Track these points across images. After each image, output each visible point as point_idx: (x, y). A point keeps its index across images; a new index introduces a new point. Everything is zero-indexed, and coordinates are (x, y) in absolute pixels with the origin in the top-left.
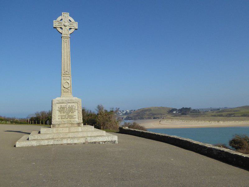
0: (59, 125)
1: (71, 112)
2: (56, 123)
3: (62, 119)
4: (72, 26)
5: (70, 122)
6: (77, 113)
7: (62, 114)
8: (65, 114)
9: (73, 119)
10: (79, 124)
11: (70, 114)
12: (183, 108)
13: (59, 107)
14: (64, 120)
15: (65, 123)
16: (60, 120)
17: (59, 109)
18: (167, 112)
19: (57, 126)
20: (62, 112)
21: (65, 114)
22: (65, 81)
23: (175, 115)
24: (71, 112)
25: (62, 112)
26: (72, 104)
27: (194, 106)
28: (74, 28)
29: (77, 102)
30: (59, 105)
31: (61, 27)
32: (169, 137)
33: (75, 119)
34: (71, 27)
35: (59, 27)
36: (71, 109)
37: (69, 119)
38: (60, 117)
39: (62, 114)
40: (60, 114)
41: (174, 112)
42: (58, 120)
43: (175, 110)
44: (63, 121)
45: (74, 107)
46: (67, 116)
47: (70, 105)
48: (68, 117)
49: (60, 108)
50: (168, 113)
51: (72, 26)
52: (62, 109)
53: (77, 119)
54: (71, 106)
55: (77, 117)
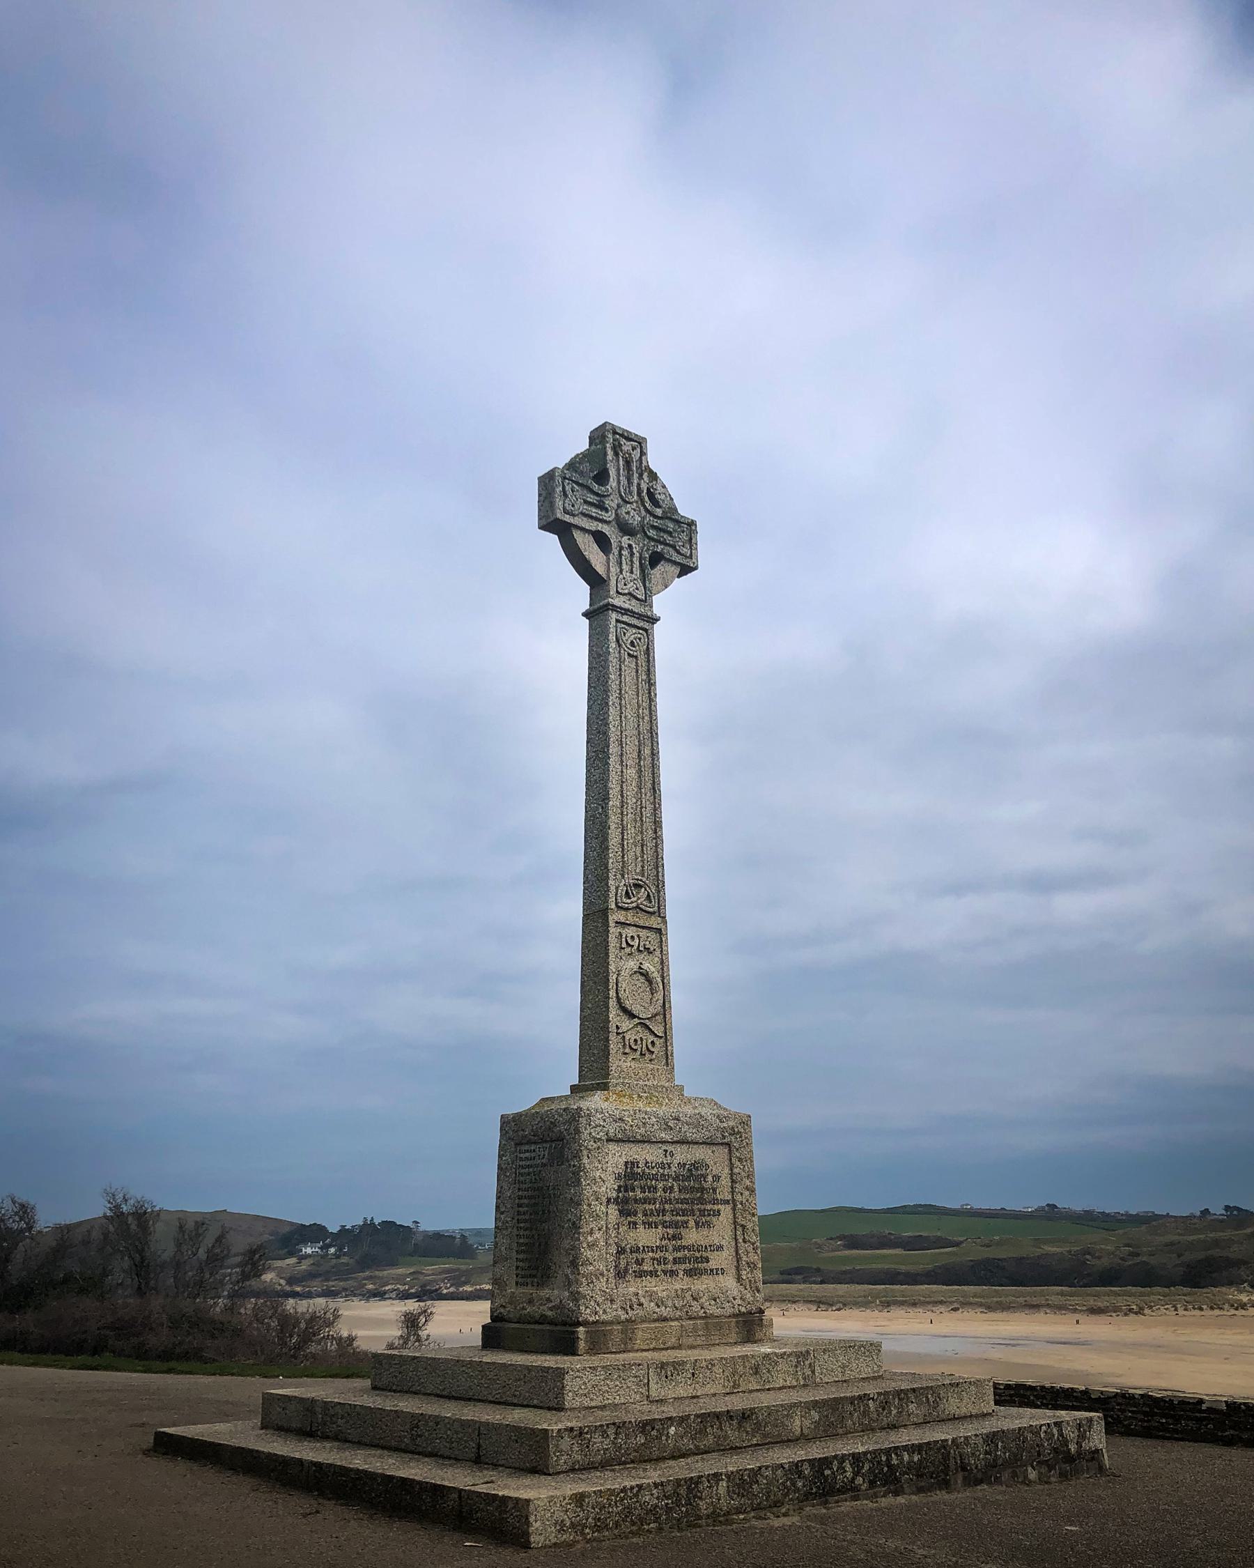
1: (691, 1223)
11: (692, 1236)
15: (664, 1311)
24: (691, 1223)
26: (700, 1153)
30: (617, 1157)
37: (680, 1283)
43: (315, 1233)
44: (651, 1295)
53: (729, 1282)
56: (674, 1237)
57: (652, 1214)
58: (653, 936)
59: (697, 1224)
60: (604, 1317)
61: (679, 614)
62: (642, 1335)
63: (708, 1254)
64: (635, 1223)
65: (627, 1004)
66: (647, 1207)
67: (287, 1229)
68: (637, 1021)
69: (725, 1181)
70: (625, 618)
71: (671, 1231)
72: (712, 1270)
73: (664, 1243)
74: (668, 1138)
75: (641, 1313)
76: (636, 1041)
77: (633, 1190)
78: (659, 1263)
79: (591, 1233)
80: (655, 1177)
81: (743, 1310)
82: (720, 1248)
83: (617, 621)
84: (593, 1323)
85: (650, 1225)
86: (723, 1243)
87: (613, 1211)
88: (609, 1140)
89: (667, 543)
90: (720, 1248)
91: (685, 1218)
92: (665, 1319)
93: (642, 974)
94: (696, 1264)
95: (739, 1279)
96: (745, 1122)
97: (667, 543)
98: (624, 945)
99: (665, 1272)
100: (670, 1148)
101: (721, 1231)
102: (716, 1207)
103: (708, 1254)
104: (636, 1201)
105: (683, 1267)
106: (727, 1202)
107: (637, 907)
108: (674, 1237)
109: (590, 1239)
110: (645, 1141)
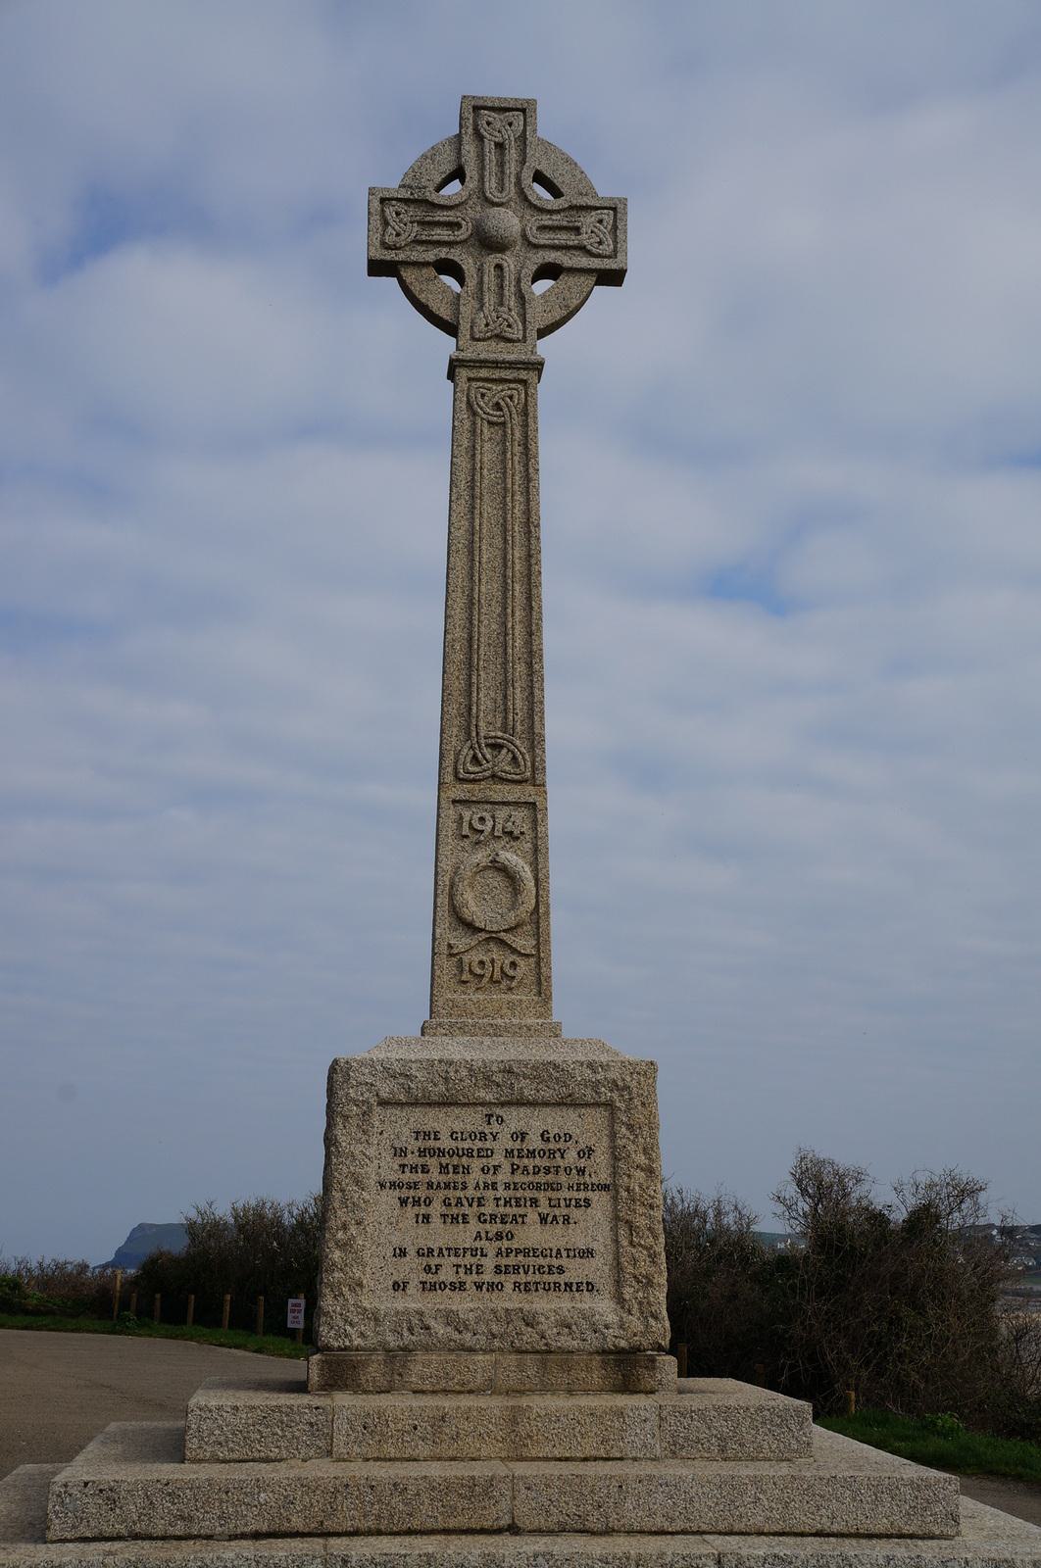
0: (397, 1357)
1: (532, 1216)
2: (372, 1341)
3: (433, 1287)
4: (570, 239)
5: (529, 1337)
6: (606, 1227)
7: (439, 1234)
8: (464, 1236)
9: (564, 1303)
10: (625, 1368)
11: (532, 1234)
13: (401, 1152)
14: (463, 1304)
17: (407, 1177)
19: (374, 1371)
20: (436, 1209)
21: (464, 1236)
22: (481, 857)
24: (532, 1216)
25: (436, 1209)
28: (584, 262)
29: (606, 1094)
31: (443, 253)
33: (586, 1302)
34: (552, 256)
35: (431, 255)
36: (541, 1178)
38: (410, 1268)
39: (439, 1234)
40: (413, 1236)
45: (571, 1156)
46: (489, 1263)
47: (535, 1123)
48: (498, 1269)
49: (412, 1159)
51: (570, 239)
52: (435, 1176)
53: (603, 1307)
54: (534, 1142)
55: (597, 1269)
56: (499, 1236)
57: (459, 1202)
59: (543, 1219)
60: (358, 1341)
61: (590, 354)
62: (420, 1368)
63: (564, 1262)
64: (427, 1218)
65: (466, 914)
66: (451, 1193)
68: (484, 935)
69: (601, 1157)
70: (484, 373)
71: (493, 1229)
72: (569, 1286)
73: (478, 1244)
74: (489, 1097)
75: (424, 1338)
76: (482, 963)
77: (425, 1170)
78: (468, 1270)
79: (345, 1227)
80: (469, 1153)
81: (623, 1344)
82: (588, 1253)
83: (470, 380)
84: (340, 1349)
85: (455, 1219)
86: (595, 1246)
87: (390, 1197)
90: (588, 1253)
91: (521, 1211)
92: (471, 1350)
93: (498, 870)
94: (542, 1273)
95: (620, 1300)
96: (648, 1071)
97: (583, 248)
98: (466, 831)
99: (479, 1286)
100: (498, 1111)
101: (593, 1226)
102: (582, 1195)
103: (564, 1262)
104: (430, 1185)
105: (513, 1278)
106: (605, 1187)
107: (493, 776)
108: (499, 1236)
109: (340, 1235)
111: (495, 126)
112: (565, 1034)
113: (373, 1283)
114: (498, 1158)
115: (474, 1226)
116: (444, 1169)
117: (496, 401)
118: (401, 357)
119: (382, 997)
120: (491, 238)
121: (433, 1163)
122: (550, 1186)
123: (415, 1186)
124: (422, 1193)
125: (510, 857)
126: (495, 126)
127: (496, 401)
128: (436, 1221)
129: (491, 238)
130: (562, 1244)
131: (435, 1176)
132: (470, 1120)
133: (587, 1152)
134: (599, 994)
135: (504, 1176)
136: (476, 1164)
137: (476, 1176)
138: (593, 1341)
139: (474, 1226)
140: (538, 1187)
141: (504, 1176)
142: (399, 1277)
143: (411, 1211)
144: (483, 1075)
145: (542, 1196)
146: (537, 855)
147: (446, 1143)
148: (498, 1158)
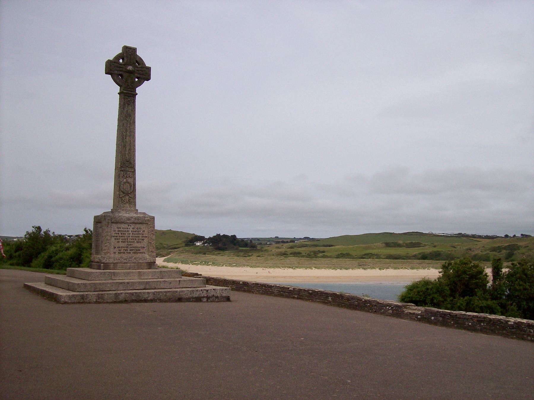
0: (115, 264)
2: (111, 262)
9: (139, 255)
11: (136, 245)
12: (218, 235)
14: (125, 256)
16: (117, 256)
17: (116, 235)
18: (184, 242)
20: (120, 240)
23: (202, 251)
25: (120, 240)
27: (242, 233)
31: (121, 73)
32: (311, 292)
39: (121, 245)
41: (198, 244)
42: (112, 255)
43: (201, 238)
50: (184, 244)
58: (131, 173)
61: (143, 91)
67: (190, 237)
69: (146, 232)
87: (113, 239)
88: (112, 223)
89: (144, 74)
94: (137, 251)
96: (154, 218)
110: (122, 223)
111: (129, 53)
112: (139, 211)
113: (110, 253)
114: (130, 232)
115: (126, 243)
116: (121, 234)
117: (128, 98)
118: (112, 90)
119: (106, 204)
120: (128, 71)
121: (120, 233)
122: (138, 237)
123: (117, 236)
124: (118, 238)
125: (130, 180)
126: (129, 53)
127: (128, 98)
128: (120, 242)
129: (128, 71)
130: (140, 246)
131: (120, 235)
132: (126, 226)
133: (144, 231)
134: (143, 204)
135: (131, 235)
136: (127, 233)
137: (127, 235)
138: (145, 261)
139: (126, 243)
140: (136, 237)
141: (131, 235)
142: (115, 251)
143: (116, 241)
144: (129, 219)
145: (137, 238)
146: (135, 179)
147: (122, 229)
148: (130, 232)
